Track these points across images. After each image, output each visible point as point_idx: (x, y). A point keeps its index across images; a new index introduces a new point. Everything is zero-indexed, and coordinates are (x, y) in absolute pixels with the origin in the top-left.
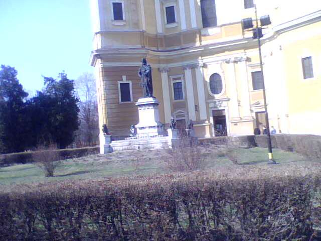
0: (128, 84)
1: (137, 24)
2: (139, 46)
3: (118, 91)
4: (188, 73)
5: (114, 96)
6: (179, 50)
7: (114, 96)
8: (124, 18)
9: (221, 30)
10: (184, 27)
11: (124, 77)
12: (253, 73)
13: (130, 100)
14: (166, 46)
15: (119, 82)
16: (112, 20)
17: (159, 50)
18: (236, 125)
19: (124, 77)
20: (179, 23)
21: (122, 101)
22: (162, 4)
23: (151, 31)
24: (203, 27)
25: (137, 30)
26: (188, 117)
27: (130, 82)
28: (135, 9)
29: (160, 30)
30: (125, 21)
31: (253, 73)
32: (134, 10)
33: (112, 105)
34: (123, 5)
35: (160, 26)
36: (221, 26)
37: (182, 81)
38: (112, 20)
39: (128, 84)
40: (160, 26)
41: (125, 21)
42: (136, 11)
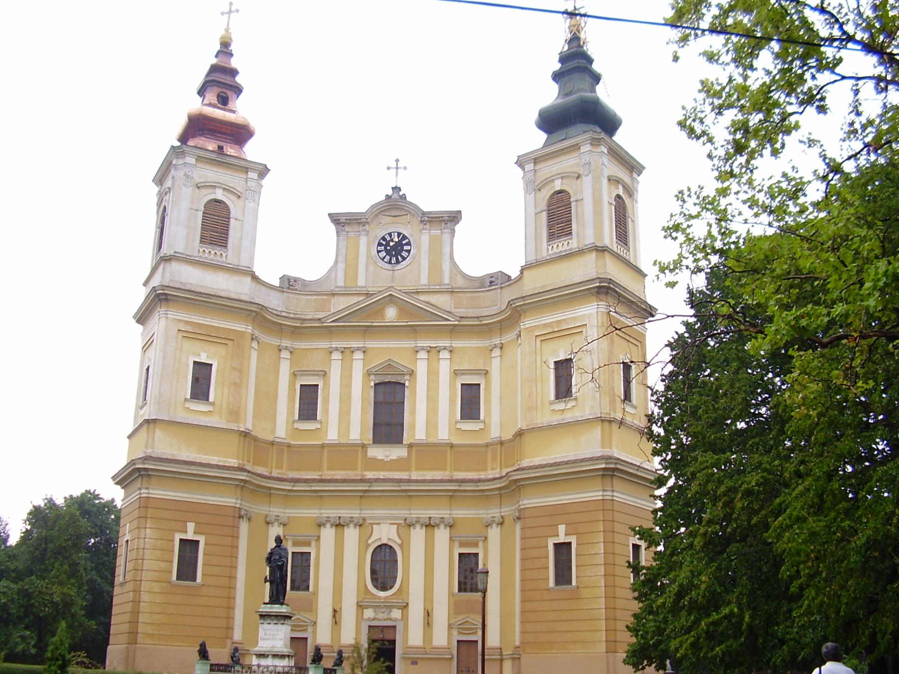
0: (197, 542)
1: (235, 414)
2: (233, 462)
3: (173, 556)
4: (328, 534)
5: (163, 565)
6: (314, 481)
7: (163, 565)
8: (211, 399)
9: (409, 453)
10: (332, 435)
11: (191, 526)
12: (460, 554)
13: (194, 579)
14: (291, 469)
15: (178, 537)
16: (186, 400)
17: (275, 474)
18: (414, 662)
19: (191, 526)
20: (325, 423)
21: (178, 579)
22: (294, 375)
23: (263, 433)
24: (374, 443)
25: (234, 426)
26: (314, 633)
27: (202, 539)
28: (237, 381)
29: (281, 432)
30: (213, 404)
31: (460, 554)
32: (235, 384)
33: (154, 584)
34: (214, 369)
35: (283, 422)
36: (410, 446)
37: (312, 550)
38: (186, 400)
39: (197, 542)
40: (283, 422)
41: (213, 404)
42: (237, 386)
